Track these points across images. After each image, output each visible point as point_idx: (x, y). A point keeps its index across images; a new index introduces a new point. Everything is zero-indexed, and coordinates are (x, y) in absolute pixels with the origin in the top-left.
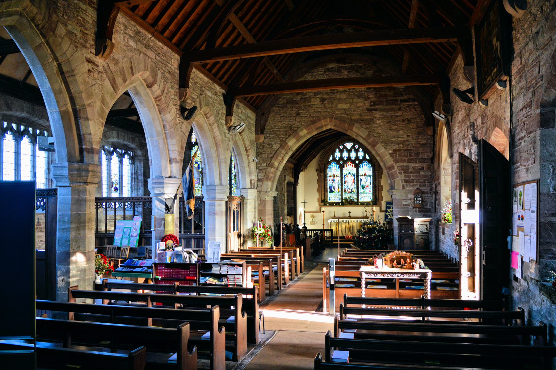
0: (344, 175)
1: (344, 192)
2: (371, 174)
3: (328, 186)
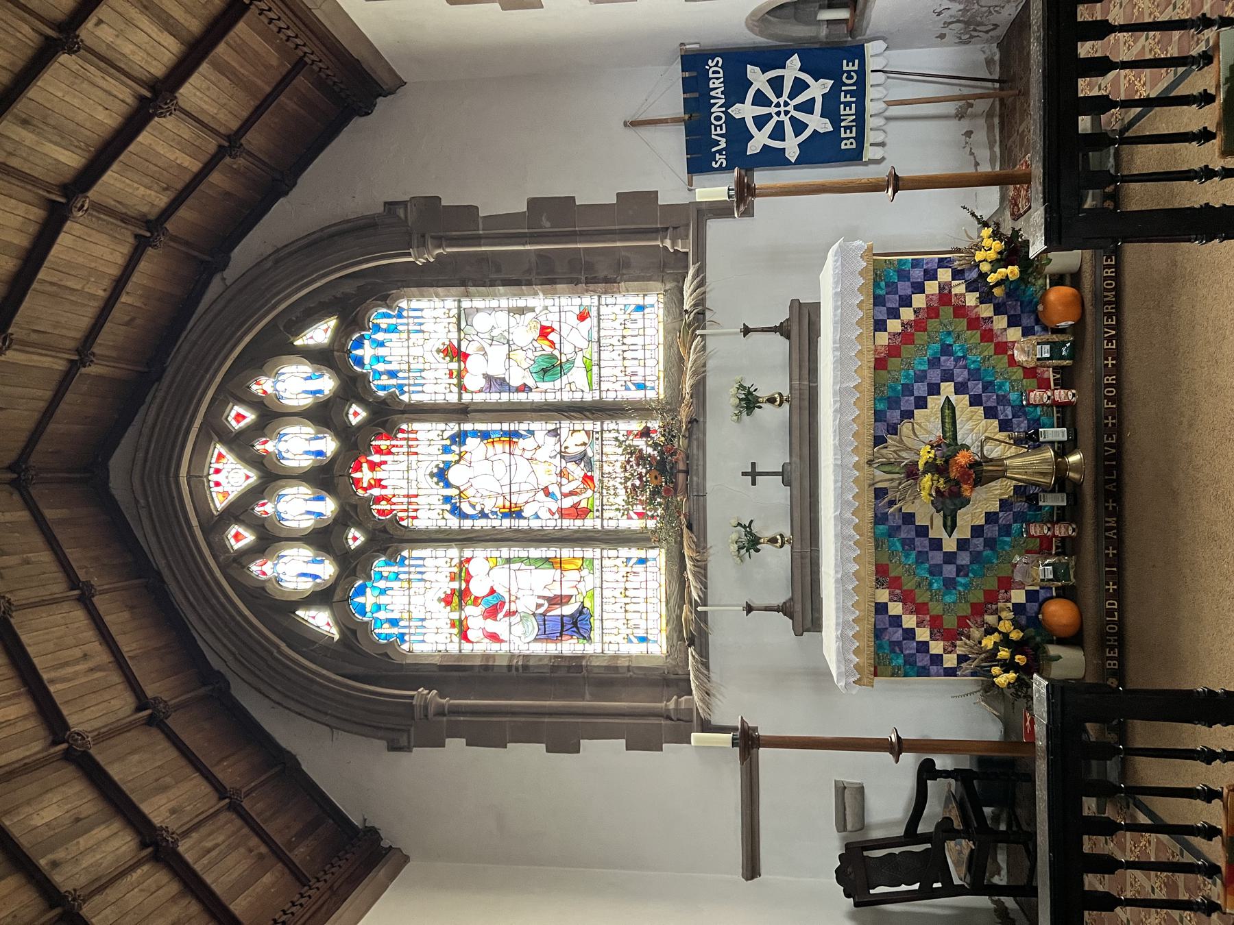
0: (454, 523)
1: (589, 523)
2: (451, 303)
3: (539, 649)
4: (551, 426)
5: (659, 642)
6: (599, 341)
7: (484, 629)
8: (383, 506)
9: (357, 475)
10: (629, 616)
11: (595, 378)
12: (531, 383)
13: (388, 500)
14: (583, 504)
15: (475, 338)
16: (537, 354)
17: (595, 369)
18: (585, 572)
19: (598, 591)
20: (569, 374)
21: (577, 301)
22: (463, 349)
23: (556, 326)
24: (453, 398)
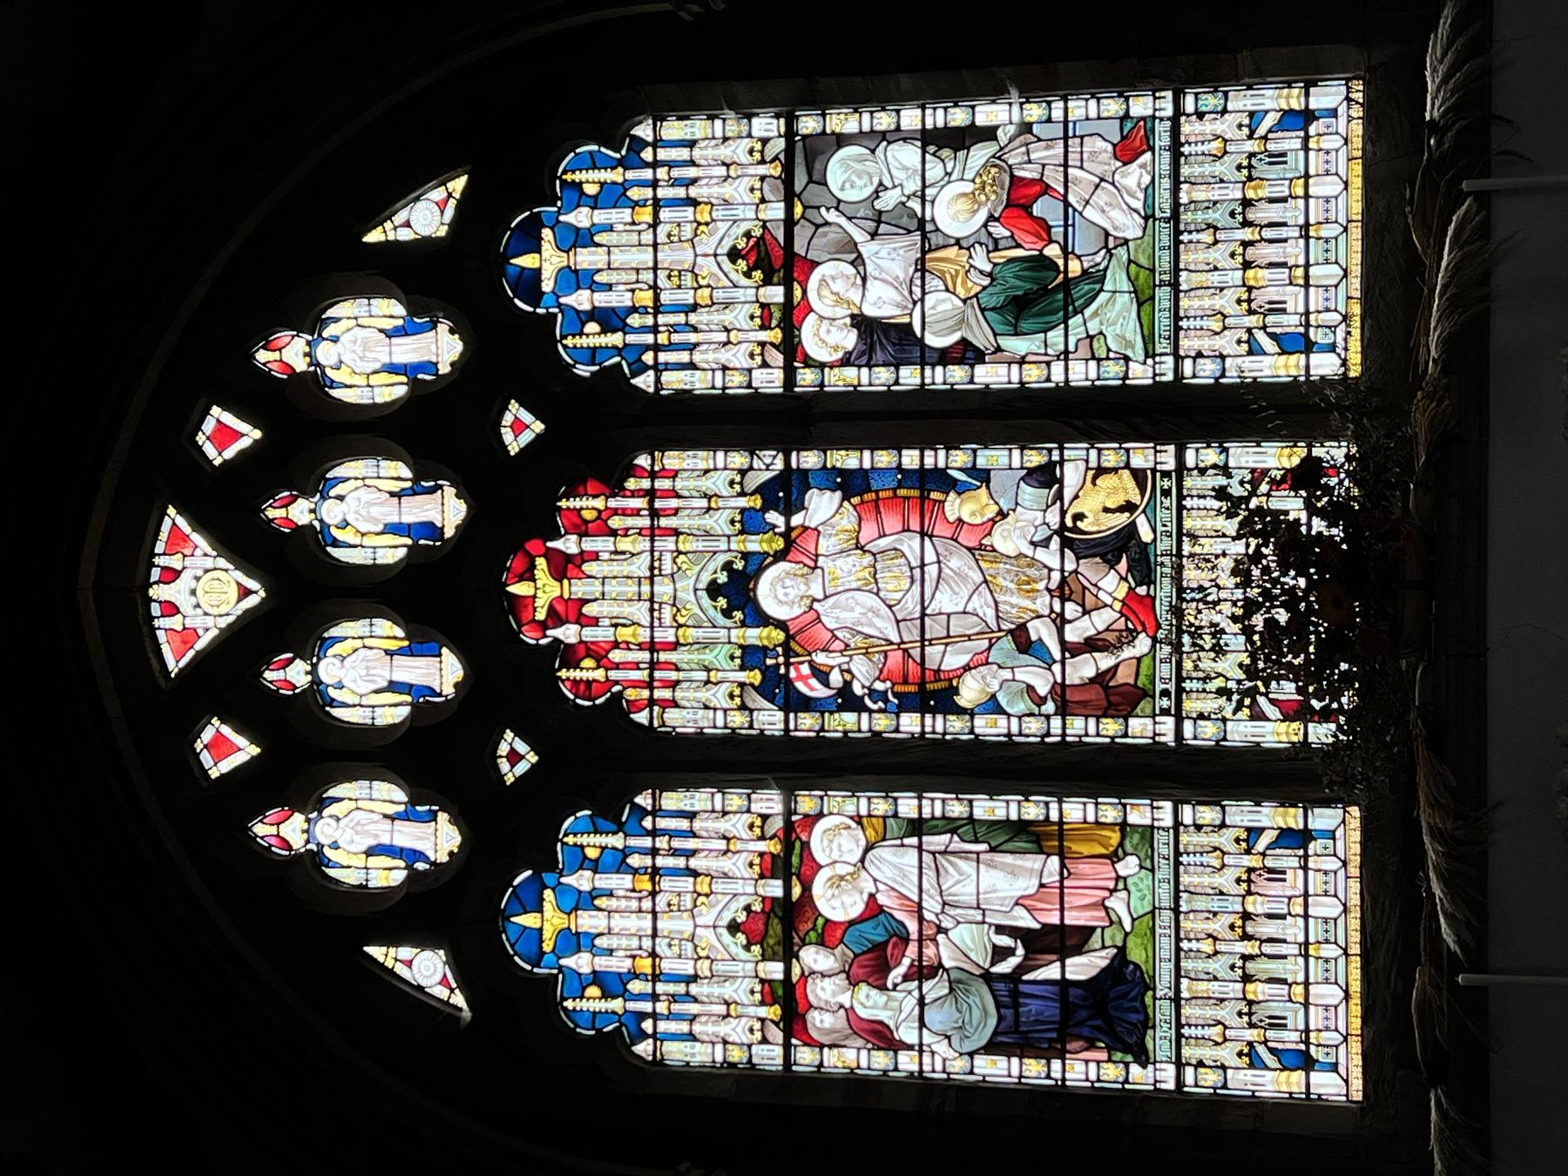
0: (770, 719)
2: (766, 125)
3: (996, 1069)
4: (1035, 458)
5: (1342, 1070)
6: (1175, 216)
7: (849, 1012)
8: (588, 671)
9: (520, 589)
10: (1257, 990)
11: (1163, 322)
12: (981, 337)
13: (601, 659)
14: (1124, 676)
15: (832, 216)
16: (1000, 257)
17: (1163, 294)
18: (1128, 866)
19: (1166, 917)
20: (1088, 312)
21: (1113, 106)
22: (799, 248)
23: (1054, 179)
24: (770, 381)
